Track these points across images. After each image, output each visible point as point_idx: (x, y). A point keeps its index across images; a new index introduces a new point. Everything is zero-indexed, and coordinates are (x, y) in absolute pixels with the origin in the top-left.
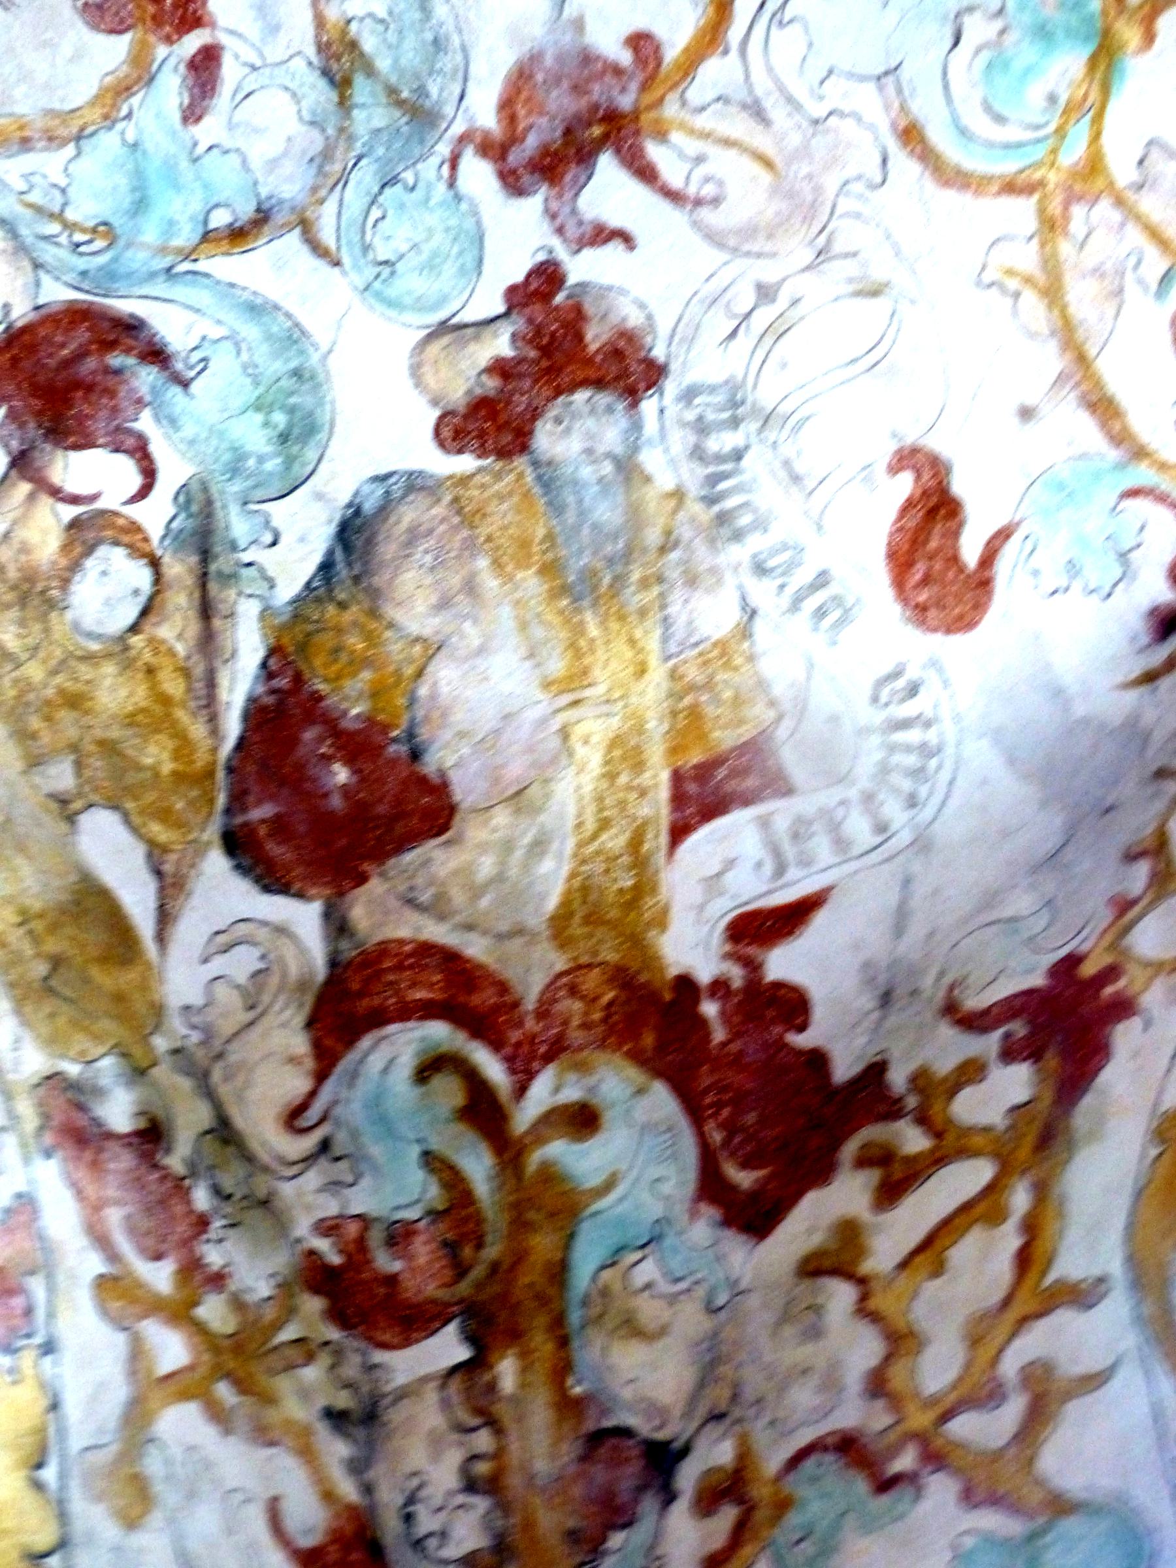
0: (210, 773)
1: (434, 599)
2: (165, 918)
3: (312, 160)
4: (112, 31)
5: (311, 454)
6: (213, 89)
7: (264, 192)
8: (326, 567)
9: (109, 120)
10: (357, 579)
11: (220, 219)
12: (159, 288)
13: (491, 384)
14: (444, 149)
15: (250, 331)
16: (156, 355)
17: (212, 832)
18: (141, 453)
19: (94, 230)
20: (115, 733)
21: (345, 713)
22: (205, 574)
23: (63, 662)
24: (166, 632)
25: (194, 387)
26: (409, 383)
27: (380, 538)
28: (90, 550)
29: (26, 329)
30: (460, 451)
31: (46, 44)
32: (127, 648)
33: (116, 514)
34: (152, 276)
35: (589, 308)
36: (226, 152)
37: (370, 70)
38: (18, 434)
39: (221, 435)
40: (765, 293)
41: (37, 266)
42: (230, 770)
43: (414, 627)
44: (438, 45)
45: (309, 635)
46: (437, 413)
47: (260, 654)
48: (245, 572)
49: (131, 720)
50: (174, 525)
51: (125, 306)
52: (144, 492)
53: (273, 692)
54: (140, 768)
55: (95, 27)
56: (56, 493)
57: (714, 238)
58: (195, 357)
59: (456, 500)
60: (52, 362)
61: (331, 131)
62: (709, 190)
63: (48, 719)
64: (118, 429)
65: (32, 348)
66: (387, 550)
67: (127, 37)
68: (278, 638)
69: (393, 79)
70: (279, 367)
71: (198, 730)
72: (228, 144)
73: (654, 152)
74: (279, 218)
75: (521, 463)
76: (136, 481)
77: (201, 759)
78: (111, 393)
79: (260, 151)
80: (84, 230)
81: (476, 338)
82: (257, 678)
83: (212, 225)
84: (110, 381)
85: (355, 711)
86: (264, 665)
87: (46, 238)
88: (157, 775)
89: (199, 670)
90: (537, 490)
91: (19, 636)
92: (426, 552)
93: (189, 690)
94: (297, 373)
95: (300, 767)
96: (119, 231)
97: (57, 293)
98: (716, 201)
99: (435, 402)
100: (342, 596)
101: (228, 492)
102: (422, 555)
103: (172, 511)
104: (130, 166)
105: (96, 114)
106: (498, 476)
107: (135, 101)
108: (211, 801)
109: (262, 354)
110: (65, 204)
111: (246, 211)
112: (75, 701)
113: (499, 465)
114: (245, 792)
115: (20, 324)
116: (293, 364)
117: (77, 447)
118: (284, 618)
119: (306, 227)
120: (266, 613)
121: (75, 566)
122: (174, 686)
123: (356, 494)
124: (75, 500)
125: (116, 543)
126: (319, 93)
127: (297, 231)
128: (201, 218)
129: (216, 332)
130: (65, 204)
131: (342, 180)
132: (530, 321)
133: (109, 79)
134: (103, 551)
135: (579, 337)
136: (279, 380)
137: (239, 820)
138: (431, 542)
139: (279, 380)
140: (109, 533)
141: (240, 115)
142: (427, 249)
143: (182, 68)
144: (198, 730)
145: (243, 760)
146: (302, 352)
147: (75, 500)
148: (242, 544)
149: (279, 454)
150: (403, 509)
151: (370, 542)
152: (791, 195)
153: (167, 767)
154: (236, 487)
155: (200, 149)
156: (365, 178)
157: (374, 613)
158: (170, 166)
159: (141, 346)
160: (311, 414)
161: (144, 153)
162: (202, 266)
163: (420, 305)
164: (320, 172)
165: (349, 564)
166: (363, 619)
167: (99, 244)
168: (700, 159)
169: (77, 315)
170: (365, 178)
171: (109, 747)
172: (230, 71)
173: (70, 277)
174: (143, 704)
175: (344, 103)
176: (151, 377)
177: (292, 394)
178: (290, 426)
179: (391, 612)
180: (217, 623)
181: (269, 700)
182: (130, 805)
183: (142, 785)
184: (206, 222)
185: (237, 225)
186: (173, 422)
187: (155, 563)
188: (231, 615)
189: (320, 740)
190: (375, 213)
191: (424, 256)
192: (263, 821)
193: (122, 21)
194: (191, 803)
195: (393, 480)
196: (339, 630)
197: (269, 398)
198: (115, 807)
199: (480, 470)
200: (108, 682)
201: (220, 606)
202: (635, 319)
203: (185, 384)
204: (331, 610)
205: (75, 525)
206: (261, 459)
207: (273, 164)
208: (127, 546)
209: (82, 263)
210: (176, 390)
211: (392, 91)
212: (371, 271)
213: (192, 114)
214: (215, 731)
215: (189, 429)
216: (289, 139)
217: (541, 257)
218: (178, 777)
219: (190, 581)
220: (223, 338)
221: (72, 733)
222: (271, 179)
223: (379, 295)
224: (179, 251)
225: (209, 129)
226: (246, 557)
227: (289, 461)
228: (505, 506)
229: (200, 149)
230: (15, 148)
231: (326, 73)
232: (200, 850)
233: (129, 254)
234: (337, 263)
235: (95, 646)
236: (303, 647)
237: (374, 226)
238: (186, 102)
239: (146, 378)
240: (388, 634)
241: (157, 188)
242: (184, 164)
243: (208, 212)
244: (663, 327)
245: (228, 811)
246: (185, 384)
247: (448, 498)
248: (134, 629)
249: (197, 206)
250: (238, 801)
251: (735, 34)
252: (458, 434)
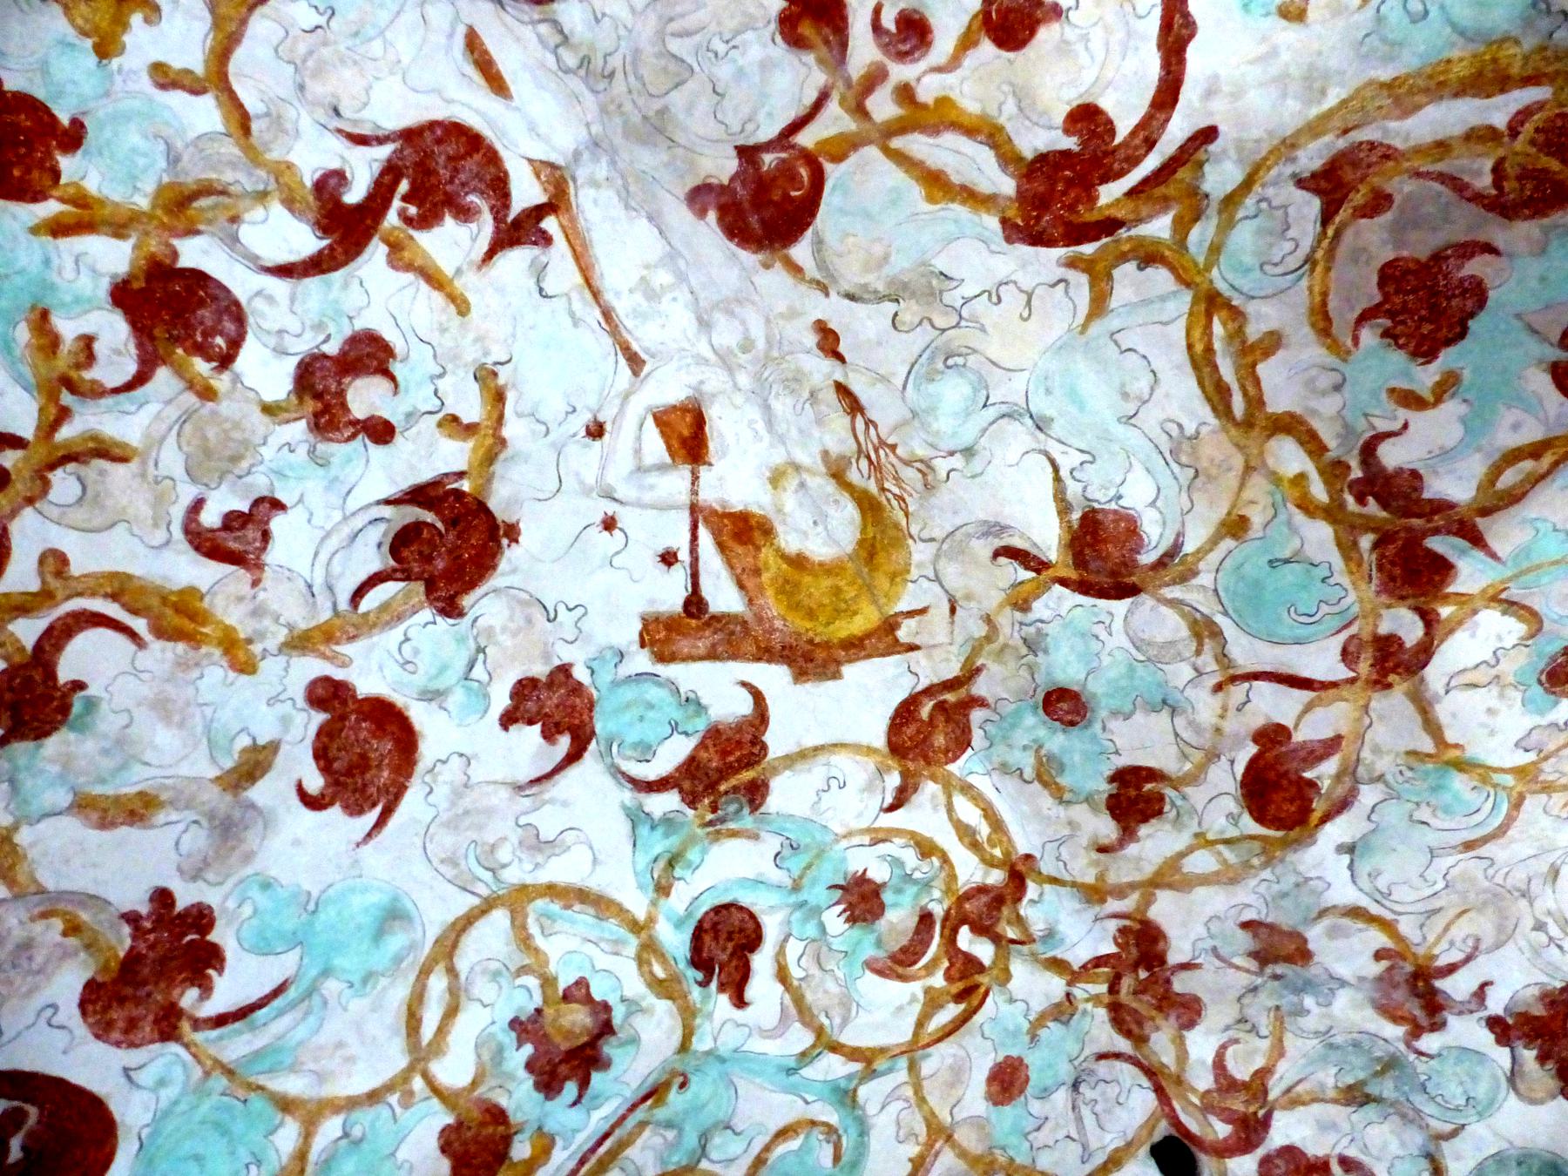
7: (1416, 1153)
13: (1550, 1065)
14: (1412, 1057)
35: (1522, 1009)
37: (1363, 1083)
40: (1540, 927)
44: (1356, 1045)
57: (1498, 946)
61: (1391, 1110)
62: (1470, 943)
69: (1371, 1072)
73: (1442, 962)
74: (1432, 1148)
79: (1394, 1148)
81: (1521, 1066)
94: (1519, 1164)
98: (1478, 940)
99: (1554, 1097)
116: (1514, 1164)
126: (1370, 1111)
131: (1418, 1112)
135: (1537, 1018)
141: (1374, 1152)
142: (1465, 1078)
152: (1485, 903)
156: (1418, 1100)
164: (1412, 1121)
168: (1452, 943)
170: (1418, 1100)
172: (1352, 1152)
175: (1378, 1100)
190: (1439, 1099)
202: (1536, 991)
207: (1403, 1144)
211: (1376, 1074)
217: (1483, 1023)
231: (1362, 1105)
234: (1463, 1126)
244: (1544, 979)
251: (1389, 916)
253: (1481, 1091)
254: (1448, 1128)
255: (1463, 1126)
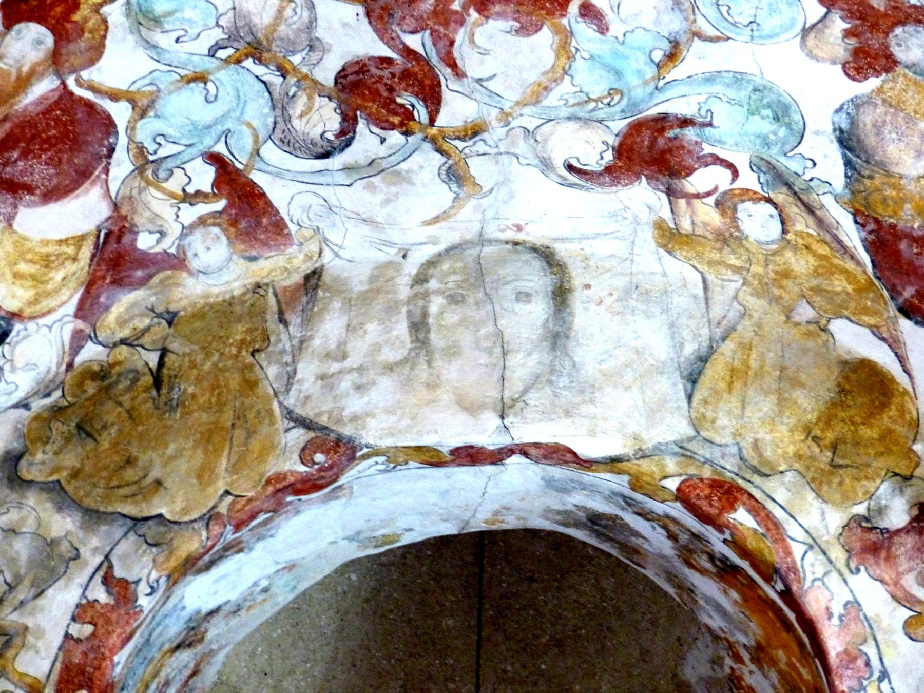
0: (872, 284)
1: (912, 154)
2: (902, 360)
3: (673, 9)
4: (537, 31)
5: (797, 117)
6: (601, 15)
8: (848, 163)
9: (571, 58)
10: (867, 162)
11: (658, 56)
12: (660, 97)
13: (853, 41)
15: (717, 88)
16: (685, 122)
17: (892, 310)
18: (718, 160)
19: (610, 94)
20: (814, 282)
21: (913, 228)
22: (795, 193)
23: (766, 260)
24: (800, 227)
25: (715, 123)
26: (813, 62)
27: (863, 136)
28: (735, 210)
29: (621, 145)
30: (866, 78)
31: (516, 54)
32: (789, 242)
33: (732, 190)
34: (651, 95)
36: (633, 31)
38: (658, 183)
39: (746, 134)
41: (600, 122)
42: (879, 278)
43: (914, 173)
45: (866, 199)
46: (840, 66)
47: (851, 217)
48: (811, 184)
49: (816, 273)
50: (762, 180)
51: (653, 112)
52: (735, 174)
53: (870, 232)
54: (838, 294)
55: (528, 35)
56: (698, 196)
58: (703, 113)
59: (884, 101)
60: (645, 150)
63: (781, 287)
64: (698, 158)
65: (631, 150)
66: (871, 140)
67: (545, 28)
68: (853, 208)
70: (743, 95)
71: (850, 266)
72: (630, 29)
74: (683, 38)
75: (899, 69)
76: (728, 173)
77: (862, 279)
78: (683, 147)
79: (648, 20)
80: (605, 97)
81: (826, 26)
82: (858, 229)
83: (657, 61)
84: (676, 143)
85: (916, 226)
86: (856, 222)
87: (594, 110)
88: (848, 294)
89: (828, 238)
90: (919, 78)
91: (737, 258)
92: (890, 133)
93: (831, 248)
94: (755, 90)
95: (910, 263)
96: (620, 88)
97: (620, 125)
99: (834, 63)
100: (867, 173)
101: (773, 154)
102: (889, 134)
103: (755, 175)
104: (598, 65)
105: (563, 60)
106: (894, 80)
107: (574, 43)
108: (882, 295)
109: (732, 93)
110: (587, 95)
111: (666, 46)
112: (786, 274)
113: (890, 76)
114: (894, 286)
115: (616, 144)
116: (750, 88)
117: (688, 175)
118: (849, 196)
119: (697, 35)
120: (837, 198)
121: (734, 219)
122: (824, 250)
123: (833, 123)
124: (708, 194)
125: (743, 201)
127: (696, 39)
128: (649, 61)
129: (702, 98)
130: (587, 95)
132: (842, 10)
133: (554, 46)
134: (741, 207)
135: (873, 8)
136: (750, 98)
137: (901, 300)
138: (889, 127)
139: (750, 98)
140: (736, 199)
143: (579, 19)
144: (850, 266)
145: (880, 271)
146: (749, 81)
147: (708, 194)
148: (800, 172)
149: (781, 126)
150: (862, 118)
151: (859, 141)
153: (850, 288)
154: (774, 151)
155: (621, 38)
157: (888, 174)
158: (616, 54)
159: (675, 123)
160: (779, 101)
161: (599, 56)
162: (669, 78)
163: (785, 29)
165: (858, 157)
166: (885, 180)
167: (617, 98)
169: (637, 127)
171: (817, 290)
173: (618, 116)
174: (816, 264)
176: (692, 132)
177: (761, 100)
178: (775, 112)
179: (896, 170)
180: (818, 213)
181: (872, 237)
182: (846, 313)
183: (844, 301)
184: (652, 61)
185: (668, 53)
186: (720, 142)
187: (769, 200)
188: (823, 206)
189: (910, 246)
190: (724, 10)
191: (766, 8)
192: (912, 297)
193: (536, 25)
194: (873, 301)
195: (845, 107)
196: (878, 190)
197: (753, 107)
198: (841, 317)
199: (884, 82)
200: (793, 260)
201: (815, 204)
203: (710, 125)
204: (866, 181)
205: (718, 204)
206: (775, 133)
207: (658, 22)
208: (749, 200)
209: (618, 108)
210: (708, 130)
212: (747, 32)
213: (603, 29)
214: (858, 263)
215: (730, 141)
216: (655, 8)
218: (860, 291)
219: (791, 199)
220: (707, 99)
221: (796, 289)
222: (663, 27)
223: (761, 37)
224: (653, 79)
225: (616, 28)
226: (807, 177)
227: (789, 126)
228: (910, 93)
229: (621, 38)
230: (545, 93)
232: (895, 322)
233: (633, 93)
234: (728, 38)
235: (774, 247)
236: (868, 206)
237: (729, 14)
238: (595, 27)
239: (690, 134)
240: (902, 182)
241: (619, 64)
242: (620, 48)
243: (650, 56)
245: (892, 298)
246: (710, 125)
247: (879, 102)
248: (784, 232)
249: (642, 58)
250: (894, 293)
252: (859, 70)
253: (768, 24)
254: (713, 33)
255: (728, 38)
